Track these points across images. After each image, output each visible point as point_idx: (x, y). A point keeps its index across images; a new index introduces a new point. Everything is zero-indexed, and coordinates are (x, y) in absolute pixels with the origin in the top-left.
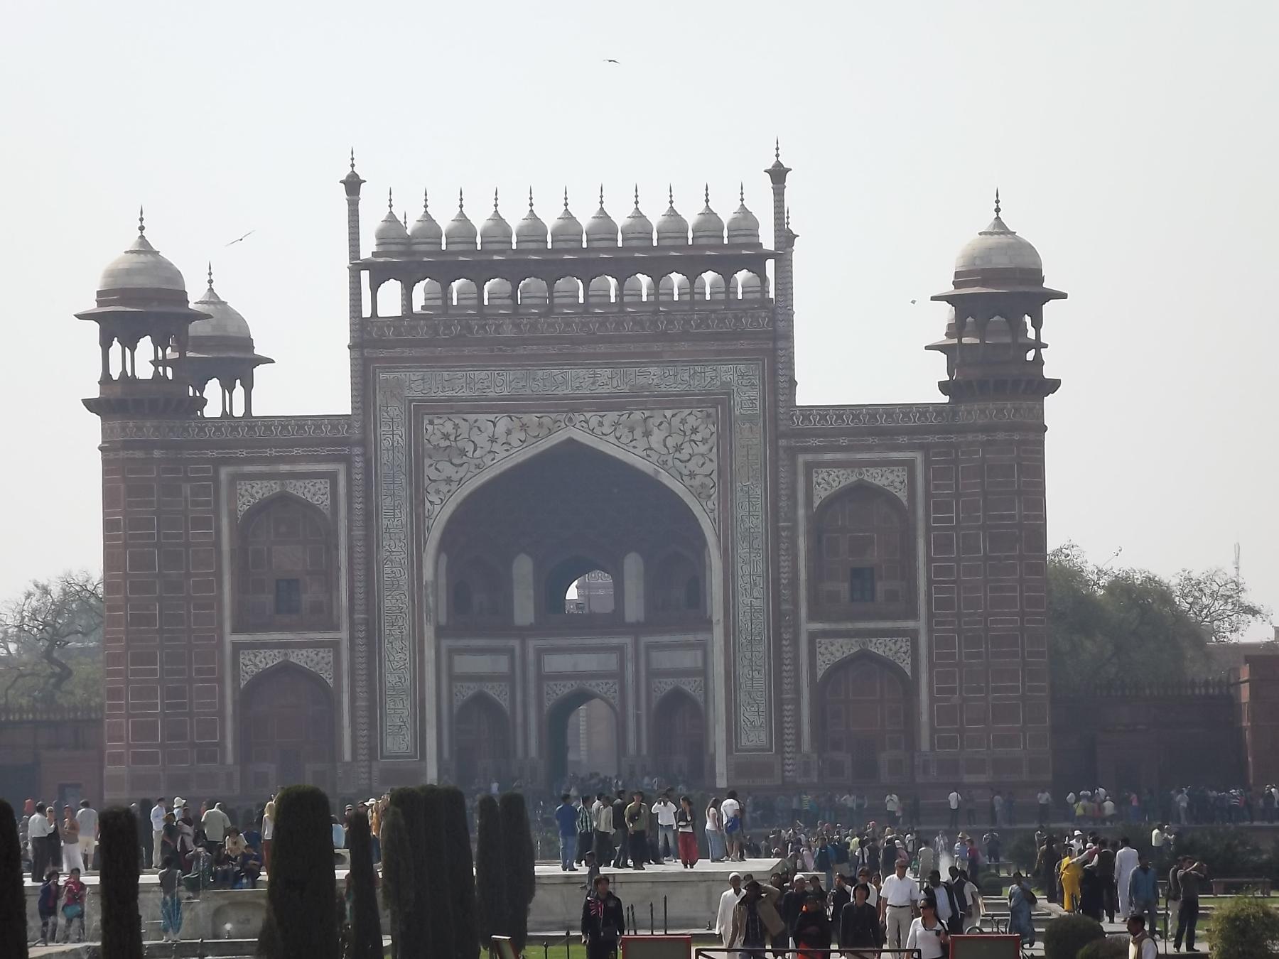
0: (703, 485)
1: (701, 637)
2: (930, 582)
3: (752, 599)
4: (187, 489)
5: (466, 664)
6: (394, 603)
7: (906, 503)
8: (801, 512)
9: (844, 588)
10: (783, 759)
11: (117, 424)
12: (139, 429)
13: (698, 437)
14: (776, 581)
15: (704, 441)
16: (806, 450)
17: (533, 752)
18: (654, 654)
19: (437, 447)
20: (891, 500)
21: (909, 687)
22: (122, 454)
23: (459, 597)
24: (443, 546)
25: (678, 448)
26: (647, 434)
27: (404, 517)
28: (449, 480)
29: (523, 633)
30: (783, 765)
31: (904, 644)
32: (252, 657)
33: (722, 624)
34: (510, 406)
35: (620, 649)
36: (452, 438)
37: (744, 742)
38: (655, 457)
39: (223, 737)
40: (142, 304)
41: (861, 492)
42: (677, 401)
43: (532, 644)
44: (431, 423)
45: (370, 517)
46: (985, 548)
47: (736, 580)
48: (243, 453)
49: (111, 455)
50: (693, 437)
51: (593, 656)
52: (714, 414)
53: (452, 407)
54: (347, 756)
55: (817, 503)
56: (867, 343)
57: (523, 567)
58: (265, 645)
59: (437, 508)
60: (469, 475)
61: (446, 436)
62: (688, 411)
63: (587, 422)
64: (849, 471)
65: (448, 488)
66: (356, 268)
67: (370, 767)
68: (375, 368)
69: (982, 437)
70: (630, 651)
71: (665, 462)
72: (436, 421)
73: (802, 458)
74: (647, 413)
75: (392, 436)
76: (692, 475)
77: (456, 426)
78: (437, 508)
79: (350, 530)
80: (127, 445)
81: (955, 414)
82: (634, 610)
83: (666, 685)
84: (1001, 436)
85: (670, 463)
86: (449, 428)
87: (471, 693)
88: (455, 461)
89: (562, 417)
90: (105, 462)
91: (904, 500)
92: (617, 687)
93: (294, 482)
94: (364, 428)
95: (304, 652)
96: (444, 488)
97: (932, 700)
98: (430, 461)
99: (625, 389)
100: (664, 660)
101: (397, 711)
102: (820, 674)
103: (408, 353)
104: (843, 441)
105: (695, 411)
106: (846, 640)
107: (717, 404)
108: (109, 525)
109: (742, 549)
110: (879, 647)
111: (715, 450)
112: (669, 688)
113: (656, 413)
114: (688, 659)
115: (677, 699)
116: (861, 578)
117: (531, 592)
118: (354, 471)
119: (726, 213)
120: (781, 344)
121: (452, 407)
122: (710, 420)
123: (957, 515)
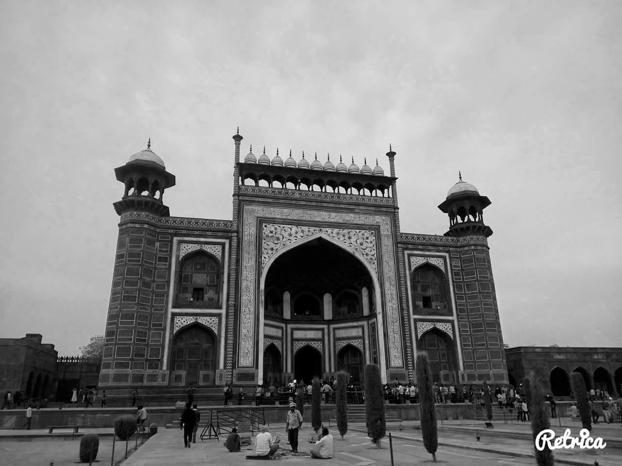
0: (371, 259)
1: (360, 323)
2: (456, 302)
3: (392, 305)
4: (157, 244)
7: (444, 272)
8: (407, 272)
9: (421, 304)
10: (409, 372)
11: (128, 213)
12: (139, 215)
13: (369, 241)
14: (401, 298)
15: (371, 242)
16: (407, 249)
17: (289, 370)
18: (337, 331)
19: (267, 236)
22: (129, 225)
25: (362, 244)
26: (350, 238)
27: (253, 263)
28: (272, 249)
29: (286, 322)
30: (409, 375)
31: (449, 325)
32: (180, 319)
33: (381, 314)
34: (298, 223)
35: (323, 330)
36: (274, 233)
37: (393, 364)
38: (353, 247)
39: (163, 357)
40: (145, 179)
41: (427, 267)
43: (290, 326)
44: (266, 226)
45: (238, 261)
46: (479, 288)
48: (184, 232)
49: (124, 227)
50: (367, 240)
51: (313, 332)
52: (374, 233)
53: (273, 221)
54: (221, 366)
55: (413, 269)
56: (421, 214)
57: (287, 296)
58: (187, 314)
59: (267, 260)
60: (280, 248)
61: (271, 232)
62: (365, 231)
63: (327, 232)
64: (423, 258)
65: (272, 252)
67: (232, 372)
68: (243, 204)
69: (473, 247)
70: (326, 331)
71: (357, 249)
72: (268, 226)
73: (406, 252)
74: (350, 230)
75: (249, 231)
76: (367, 255)
77: (276, 229)
78: (267, 260)
79: (229, 266)
80: (132, 222)
81: (458, 241)
83: (343, 344)
84: (479, 248)
85: (359, 249)
86: (273, 229)
87: (270, 343)
88: (275, 242)
89: (317, 229)
90: (120, 230)
91: (443, 270)
92: (321, 345)
93: (206, 245)
94: (238, 226)
95: (205, 318)
96: (270, 252)
97: (462, 349)
98: (265, 241)
99: (341, 221)
100: (341, 334)
101: (246, 346)
102: (419, 337)
103: (257, 199)
104: (420, 247)
105: (367, 231)
106: (428, 323)
107: (376, 229)
108: (119, 257)
109: (387, 285)
110: (440, 326)
111: (375, 246)
112: (344, 345)
113: (353, 230)
116: (427, 302)
117: (290, 306)
118: (232, 243)
119: (372, 166)
120: (396, 211)
121: (273, 221)
122: (373, 235)
123: (463, 277)
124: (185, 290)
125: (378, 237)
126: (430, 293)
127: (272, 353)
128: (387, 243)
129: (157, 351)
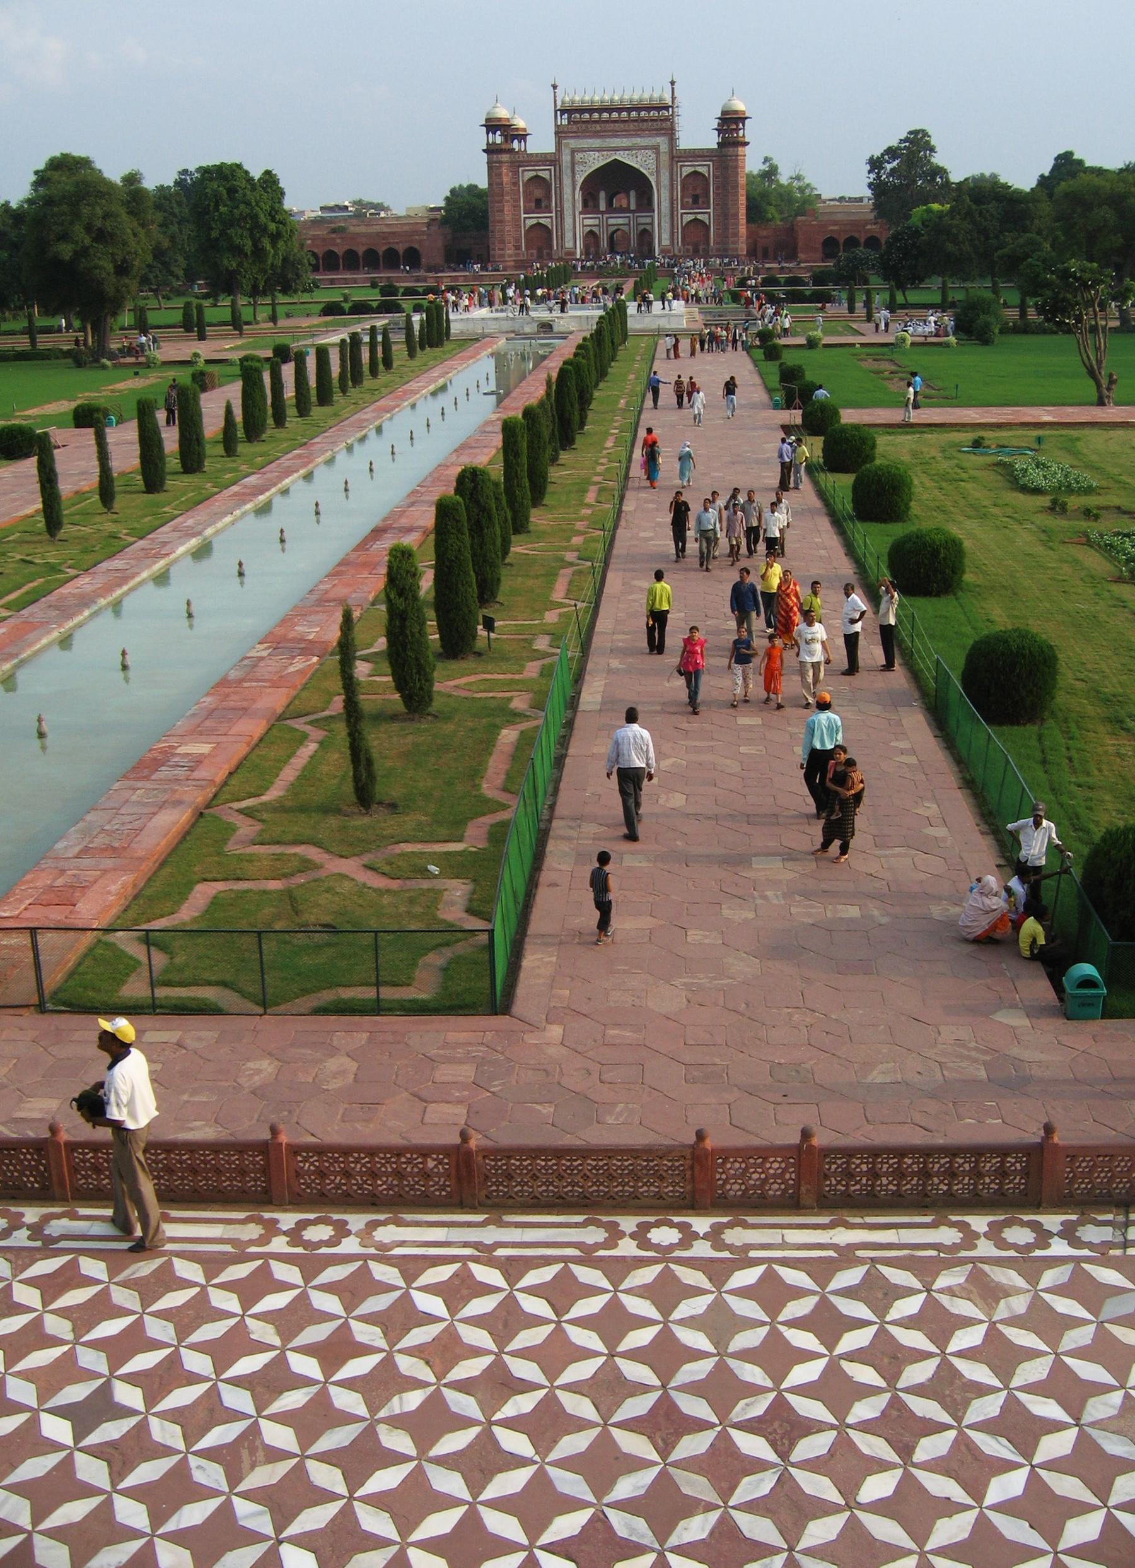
3: (665, 205)
5: (587, 222)
6: (567, 206)
20: (703, 176)
21: (707, 228)
23: (585, 203)
24: (581, 189)
29: (603, 213)
34: (599, 150)
41: (695, 173)
42: (645, 148)
47: (662, 198)
53: (582, 150)
57: (602, 195)
66: (556, 112)
75: (566, 158)
82: (633, 207)
83: (642, 227)
101: (569, 235)
107: (656, 149)
109: (663, 190)
110: (699, 217)
114: (648, 220)
115: (645, 231)
116: (696, 199)
121: (582, 150)
124: (530, 201)
125: (658, 153)
126: (698, 192)
127: (591, 237)
128: (665, 158)
129: (518, 240)
